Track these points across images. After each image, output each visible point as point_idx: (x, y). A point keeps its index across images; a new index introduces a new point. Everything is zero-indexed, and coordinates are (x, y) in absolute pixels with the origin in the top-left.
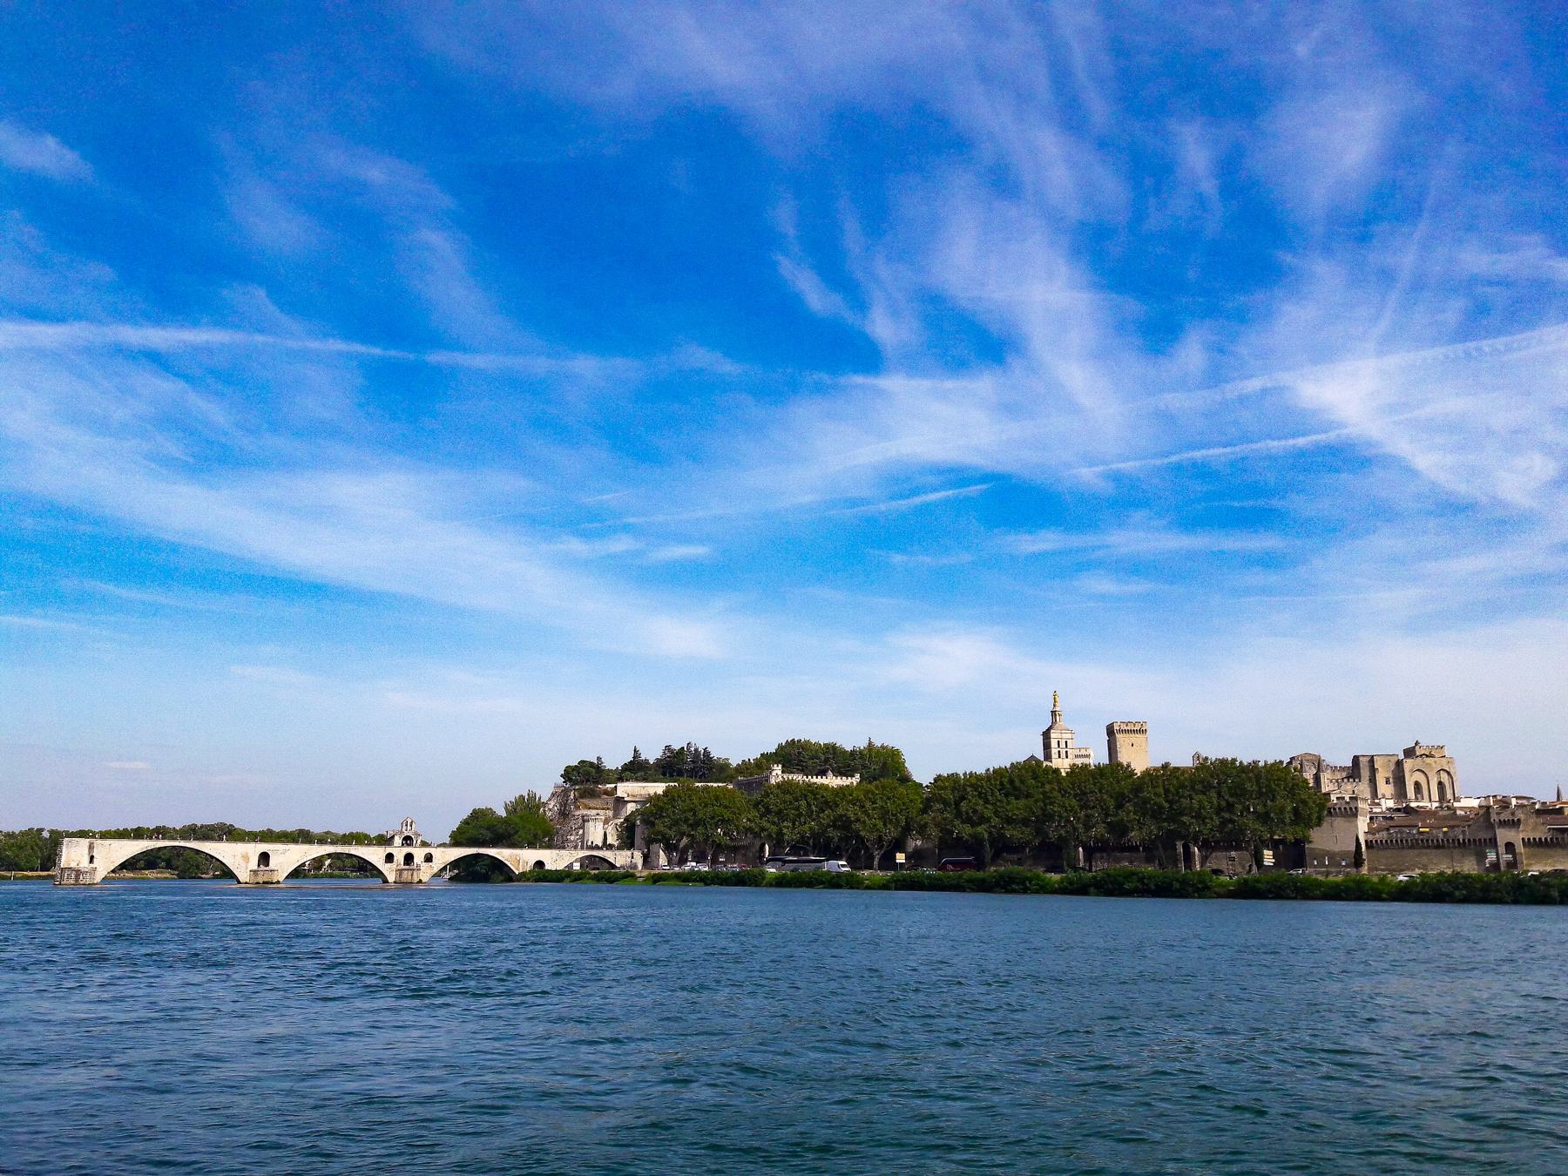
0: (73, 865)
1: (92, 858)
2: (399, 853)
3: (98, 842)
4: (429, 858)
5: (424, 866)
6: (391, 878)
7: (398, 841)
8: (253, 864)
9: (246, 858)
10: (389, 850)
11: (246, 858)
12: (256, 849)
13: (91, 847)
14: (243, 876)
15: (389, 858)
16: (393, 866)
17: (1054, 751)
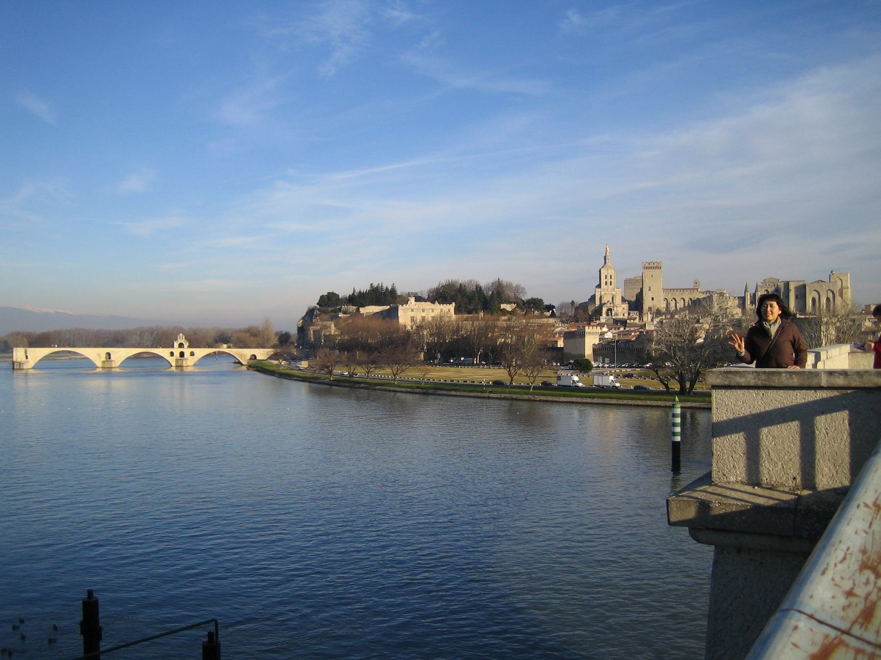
0: (19, 360)
1: (27, 357)
2: (177, 351)
3: (29, 349)
4: (192, 354)
5: (190, 358)
6: (174, 364)
7: (176, 344)
8: (103, 358)
9: (99, 355)
10: (171, 350)
11: (99, 355)
12: (103, 351)
13: (26, 352)
14: (99, 364)
15: (172, 354)
16: (174, 358)
17: (603, 280)
